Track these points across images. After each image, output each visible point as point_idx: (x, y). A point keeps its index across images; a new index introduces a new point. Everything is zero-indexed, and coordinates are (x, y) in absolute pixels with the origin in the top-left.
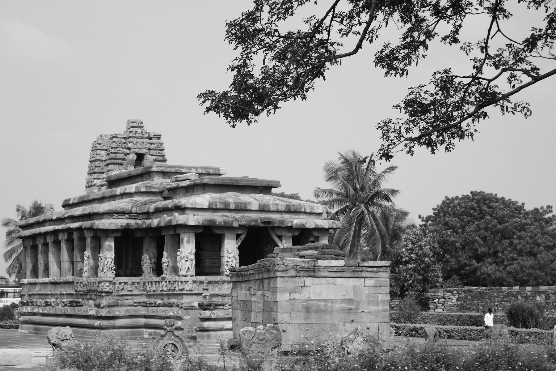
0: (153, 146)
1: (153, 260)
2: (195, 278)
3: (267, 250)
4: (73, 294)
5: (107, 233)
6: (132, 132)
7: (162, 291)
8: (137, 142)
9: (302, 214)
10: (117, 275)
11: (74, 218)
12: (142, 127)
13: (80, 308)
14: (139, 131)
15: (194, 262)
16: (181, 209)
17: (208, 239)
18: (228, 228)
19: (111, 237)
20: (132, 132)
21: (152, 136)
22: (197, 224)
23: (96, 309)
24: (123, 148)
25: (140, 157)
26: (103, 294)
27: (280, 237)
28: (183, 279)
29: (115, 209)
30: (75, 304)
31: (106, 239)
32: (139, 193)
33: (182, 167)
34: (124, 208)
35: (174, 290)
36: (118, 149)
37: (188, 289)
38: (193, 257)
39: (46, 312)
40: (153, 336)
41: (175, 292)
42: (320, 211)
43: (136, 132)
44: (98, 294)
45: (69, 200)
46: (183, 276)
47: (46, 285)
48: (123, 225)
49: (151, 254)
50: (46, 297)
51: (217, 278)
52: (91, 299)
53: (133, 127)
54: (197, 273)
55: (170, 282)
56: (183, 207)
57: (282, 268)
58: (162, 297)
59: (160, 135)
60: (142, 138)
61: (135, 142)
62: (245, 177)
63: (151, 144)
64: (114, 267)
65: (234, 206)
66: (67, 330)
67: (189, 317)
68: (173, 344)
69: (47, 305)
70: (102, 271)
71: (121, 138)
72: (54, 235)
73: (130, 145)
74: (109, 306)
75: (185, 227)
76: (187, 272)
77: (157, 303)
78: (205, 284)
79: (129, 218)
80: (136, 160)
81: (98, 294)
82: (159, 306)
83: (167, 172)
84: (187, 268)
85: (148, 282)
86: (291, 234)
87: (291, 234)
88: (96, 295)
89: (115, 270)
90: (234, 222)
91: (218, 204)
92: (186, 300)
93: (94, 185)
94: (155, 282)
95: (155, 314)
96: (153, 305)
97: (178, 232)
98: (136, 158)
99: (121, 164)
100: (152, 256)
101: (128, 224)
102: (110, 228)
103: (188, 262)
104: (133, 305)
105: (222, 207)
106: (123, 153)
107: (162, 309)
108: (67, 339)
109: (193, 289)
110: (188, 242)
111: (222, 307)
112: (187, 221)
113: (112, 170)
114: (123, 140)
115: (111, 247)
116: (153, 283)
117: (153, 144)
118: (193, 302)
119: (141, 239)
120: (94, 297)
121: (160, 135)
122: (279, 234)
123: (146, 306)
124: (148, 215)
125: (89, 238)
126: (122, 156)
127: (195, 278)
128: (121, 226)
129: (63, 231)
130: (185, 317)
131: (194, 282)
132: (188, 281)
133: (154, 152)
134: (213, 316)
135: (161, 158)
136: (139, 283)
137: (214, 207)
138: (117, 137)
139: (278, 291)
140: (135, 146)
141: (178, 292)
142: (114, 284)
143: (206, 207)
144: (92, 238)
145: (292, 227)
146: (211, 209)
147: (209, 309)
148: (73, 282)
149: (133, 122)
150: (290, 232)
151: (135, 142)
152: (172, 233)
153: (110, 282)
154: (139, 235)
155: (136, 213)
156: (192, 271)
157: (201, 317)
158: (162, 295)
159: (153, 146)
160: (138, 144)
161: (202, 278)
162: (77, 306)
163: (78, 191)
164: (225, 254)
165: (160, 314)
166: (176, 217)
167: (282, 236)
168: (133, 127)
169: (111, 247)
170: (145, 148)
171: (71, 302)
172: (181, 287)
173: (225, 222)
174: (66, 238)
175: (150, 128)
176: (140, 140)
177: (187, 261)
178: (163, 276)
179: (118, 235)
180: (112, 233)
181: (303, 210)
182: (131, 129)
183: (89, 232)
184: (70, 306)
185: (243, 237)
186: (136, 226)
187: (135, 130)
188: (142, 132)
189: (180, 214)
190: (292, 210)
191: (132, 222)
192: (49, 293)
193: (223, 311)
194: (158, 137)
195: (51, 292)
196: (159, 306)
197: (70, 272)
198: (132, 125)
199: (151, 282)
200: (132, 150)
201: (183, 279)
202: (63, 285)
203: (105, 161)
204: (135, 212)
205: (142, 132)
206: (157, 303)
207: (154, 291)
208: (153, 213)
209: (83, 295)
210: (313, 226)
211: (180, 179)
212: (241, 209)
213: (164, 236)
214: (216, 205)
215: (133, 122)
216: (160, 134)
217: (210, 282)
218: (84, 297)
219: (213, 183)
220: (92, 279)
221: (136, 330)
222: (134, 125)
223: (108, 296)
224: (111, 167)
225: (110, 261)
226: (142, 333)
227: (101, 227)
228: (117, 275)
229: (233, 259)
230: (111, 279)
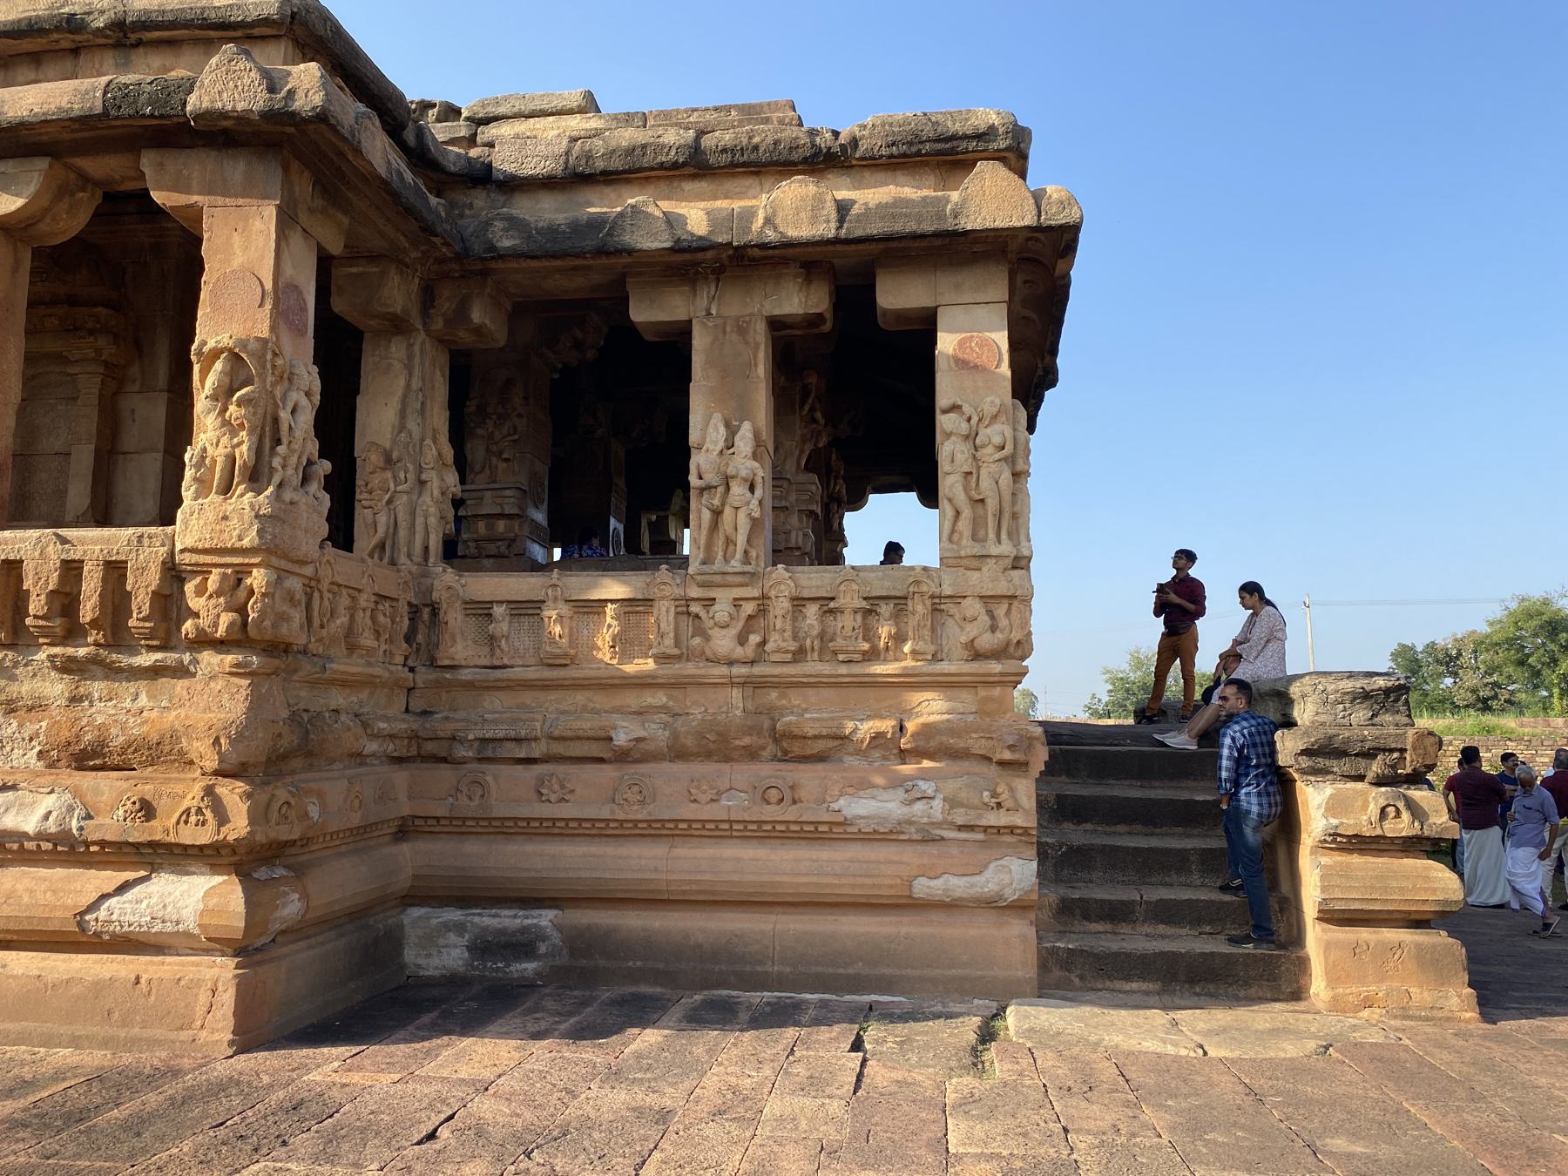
82: (623, 757)
96: (537, 751)
115: (304, 309)
152: (797, 300)
206: (621, 739)
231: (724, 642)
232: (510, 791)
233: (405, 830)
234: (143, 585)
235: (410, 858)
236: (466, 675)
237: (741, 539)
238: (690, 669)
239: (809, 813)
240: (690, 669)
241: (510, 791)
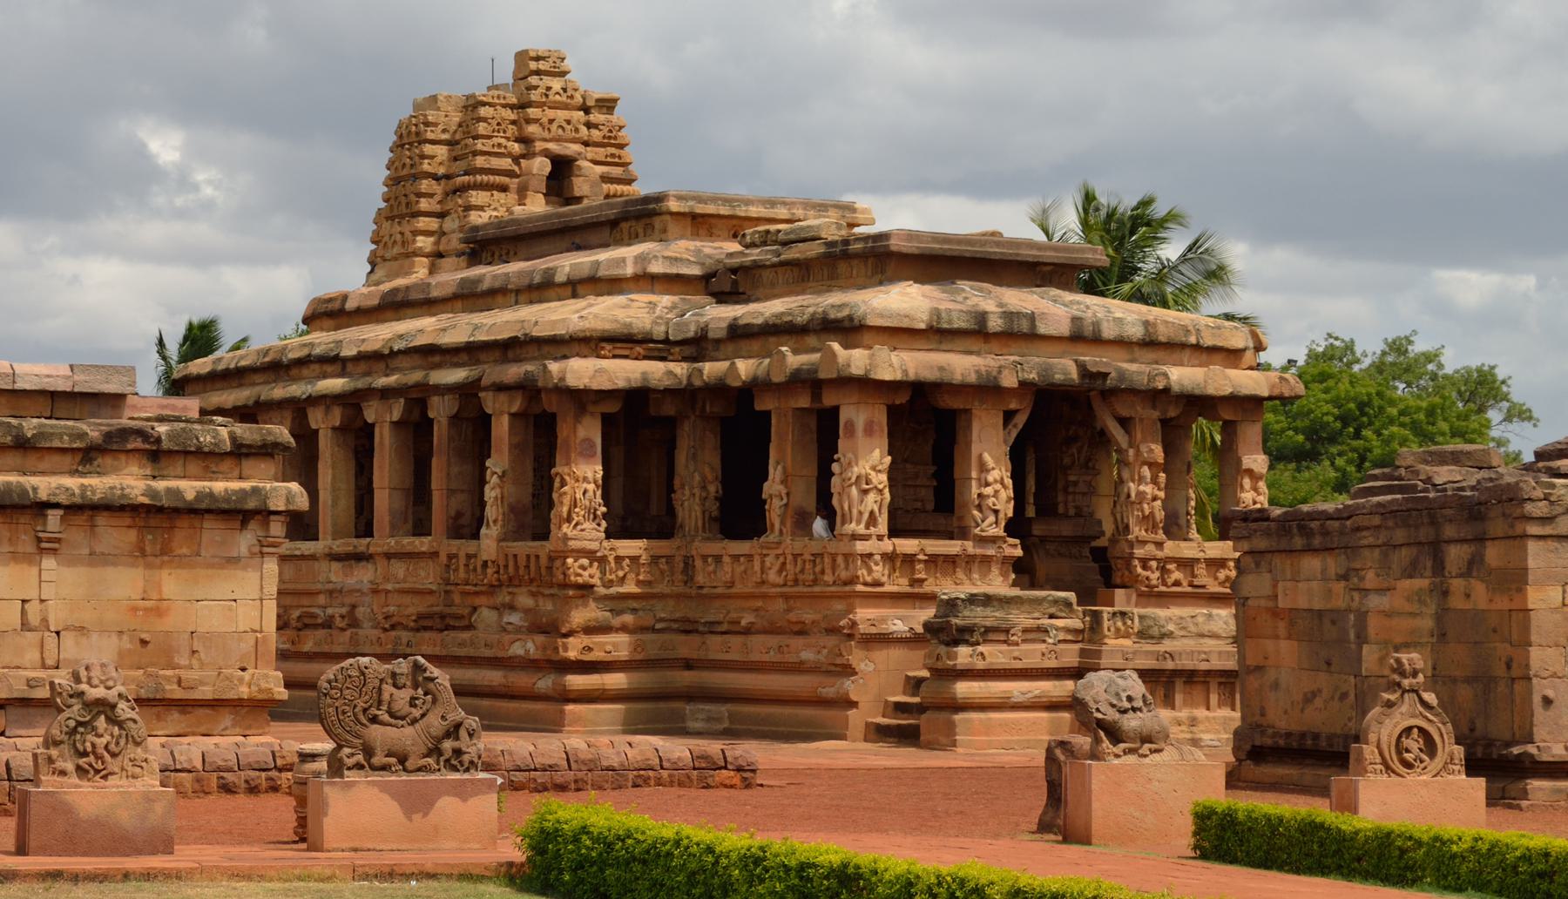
0: (596, 135)
1: (712, 489)
2: (888, 545)
3: (1067, 461)
4: (431, 592)
5: (582, 399)
6: (536, 88)
7: (763, 582)
8: (551, 121)
9: (1187, 354)
10: (609, 535)
11: (333, 362)
12: (563, 74)
13: (466, 635)
14: (556, 84)
16: (850, 329)
17: (927, 424)
18: (988, 390)
19: (592, 414)
20: (536, 88)
21: (590, 103)
22: (899, 376)
23: (540, 639)
24: (508, 139)
25: (562, 168)
26: (571, 593)
27: (1125, 423)
28: (860, 547)
29: (608, 326)
30: (437, 623)
31: (578, 418)
32: (646, 281)
33: (748, 202)
34: (630, 324)
35: (815, 582)
36: (495, 140)
37: (869, 579)
38: (884, 477)
39: (308, 646)
40: (726, 725)
41: (817, 589)
42: (1241, 345)
43: (549, 89)
44: (547, 592)
45: (345, 297)
46: (855, 537)
47: (303, 564)
48: (632, 376)
49: (707, 469)
50: (305, 601)
51: (952, 547)
52: (512, 607)
53: (538, 73)
54: (894, 532)
55: (795, 556)
56: (856, 322)
57: (1539, 509)
58: (759, 603)
59: (615, 101)
60: (566, 107)
61: (545, 120)
62: (993, 234)
63: (589, 125)
64: (604, 509)
65: (1000, 321)
66: (1130, 682)
67: (871, 667)
68: (1421, 729)
69: (306, 626)
70: (569, 520)
71: (504, 106)
72: (344, 405)
73: (532, 129)
74: (589, 630)
75: (866, 385)
76: (867, 527)
77: (743, 623)
78: (919, 566)
79: (646, 358)
80: (550, 177)
81: (547, 592)
83: (703, 216)
84: (866, 516)
85: (704, 558)
86: (1156, 414)
87: (1156, 414)
88: (533, 595)
89: (605, 516)
90: (1006, 372)
91: (955, 315)
92: (865, 615)
93: (415, 254)
94: (736, 558)
95: (734, 656)
96: (725, 627)
97: (829, 400)
98: (548, 169)
99: (504, 189)
100: (710, 477)
101: (644, 373)
102: (595, 386)
103: (872, 497)
104: (654, 630)
105: (964, 325)
106: (509, 155)
107: (773, 641)
108: (1134, 709)
109: (884, 579)
110: (869, 430)
111: (1002, 637)
112: (873, 365)
113: (481, 208)
114: (511, 115)
115: (593, 446)
116: (726, 559)
117: (596, 126)
118: (883, 620)
119: (671, 424)
120: (525, 600)
121: (615, 101)
122: (1125, 413)
123: (697, 631)
124: (698, 346)
125: (505, 419)
126: (506, 163)
127: (888, 545)
128: (629, 380)
129: (386, 394)
130: (862, 666)
131: (889, 558)
132: (870, 555)
133: (600, 153)
134: (980, 665)
135: (616, 171)
136: (669, 559)
137: (945, 326)
138: (490, 105)
139: (1530, 577)
140: (546, 135)
141: (833, 589)
142: (603, 560)
143: (923, 326)
144: (512, 415)
145: (1167, 390)
146: (937, 334)
147: (967, 643)
148: (434, 555)
149: (538, 59)
150: (1154, 407)
151: (545, 120)
152: (804, 402)
153: (590, 554)
154: (669, 409)
155: (666, 341)
156: (883, 526)
157: (939, 665)
158: (764, 596)
159: (596, 135)
160: (554, 127)
161: (908, 545)
162: (448, 628)
163: (348, 273)
164: (974, 474)
165: (755, 657)
166: (834, 355)
167: (1131, 418)
168: (538, 73)
169: (588, 441)
170: (574, 141)
171: (420, 617)
172: (844, 575)
173: (977, 372)
174: (396, 416)
175: (587, 77)
176: (561, 115)
177: (866, 492)
178: (771, 537)
179: (613, 407)
180: (595, 403)
181: (1193, 340)
182: (534, 80)
183: (503, 397)
184: (418, 630)
185: (1021, 420)
186: (668, 382)
187: (548, 81)
188: (565, 90)
189: (846, 346)
190: (1162, 339)
191: (656, 371)
192: (319, 586)
193: (1004, 647)
194: (608, 105)
195: (330, 586)
196: (747, 631)
197: (406, 521)
198: (533, 65)
199: (718, 559)
200: (539, 146)
201: (860, 547)
202: (381, 563)
203: (448, 177)
204: (662, 337)
205: (565, 90)
206: (743, 623)
207: (732, 584)
208: (718, 341)
209: (476, 593)
210: (1228, 391)
211: (781, 236)
212: (1019, 333)
213: (767, 415)
214: (950, 322)
215: (538, 59)
216: (615, 95)
217: (933, 561)
218: (482, 600)
219: (916, 252)
220: (524, 548)
221: (662, 705)
222: (542, 66)
223: (583, 596)
224: (477, 197)
225: (591, 487)
226: (683, 719)
227: (572, 381)
228: (609, 535)
229: (998, 486)
230: (594, 546)
231: (772, 576)
232: (715, 647)
233: (689, 665)
234: (544, 561)
235: (686, 678)
236: (705, 591)
237: (777, 526)
238: (764, 589)
239: (791, 658)
240: (764, 589)
241: (715, 647)
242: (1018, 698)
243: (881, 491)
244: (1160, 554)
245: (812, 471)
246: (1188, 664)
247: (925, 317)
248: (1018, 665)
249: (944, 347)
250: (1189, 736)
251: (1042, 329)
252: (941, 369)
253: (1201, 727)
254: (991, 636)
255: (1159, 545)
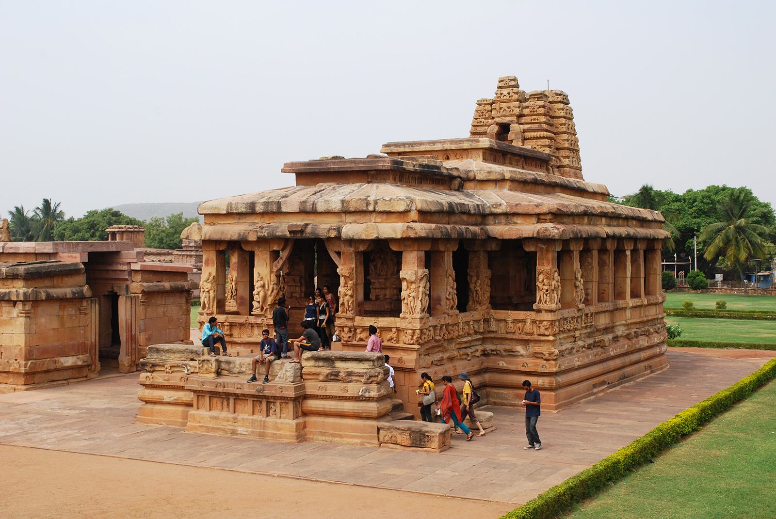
15: (211, 292)
27: (339, 254)
33: (421, 144)
60: (510, 101)
65: (262, 207)
86: (352, 250)
91: (239, 205)
105: (244, 210)
111: (163, 369)
114: (488, 107)
137: (234, 211)
150: (351, 246)
176: (504, 105)
181: (371, 208)
193: (164, 374)
214: (237, 209)
219: (303, 171)
242: (167, 400)
243: (208, 292)
244: (350, 324)
245: (247, 279)
246: (230, 390)
247: (225, 208)
248: (166, 383)
249: (241, 221)
250: (231, 427)
251: (284, 209)
252: (223, 233)
253: (239, 424)
254: (157, 368)
255: (352, 319)
